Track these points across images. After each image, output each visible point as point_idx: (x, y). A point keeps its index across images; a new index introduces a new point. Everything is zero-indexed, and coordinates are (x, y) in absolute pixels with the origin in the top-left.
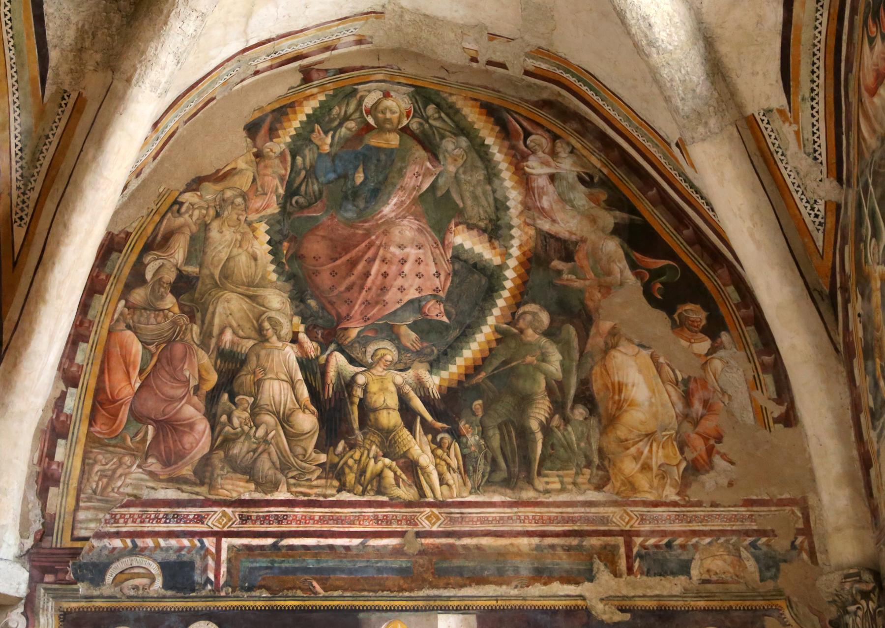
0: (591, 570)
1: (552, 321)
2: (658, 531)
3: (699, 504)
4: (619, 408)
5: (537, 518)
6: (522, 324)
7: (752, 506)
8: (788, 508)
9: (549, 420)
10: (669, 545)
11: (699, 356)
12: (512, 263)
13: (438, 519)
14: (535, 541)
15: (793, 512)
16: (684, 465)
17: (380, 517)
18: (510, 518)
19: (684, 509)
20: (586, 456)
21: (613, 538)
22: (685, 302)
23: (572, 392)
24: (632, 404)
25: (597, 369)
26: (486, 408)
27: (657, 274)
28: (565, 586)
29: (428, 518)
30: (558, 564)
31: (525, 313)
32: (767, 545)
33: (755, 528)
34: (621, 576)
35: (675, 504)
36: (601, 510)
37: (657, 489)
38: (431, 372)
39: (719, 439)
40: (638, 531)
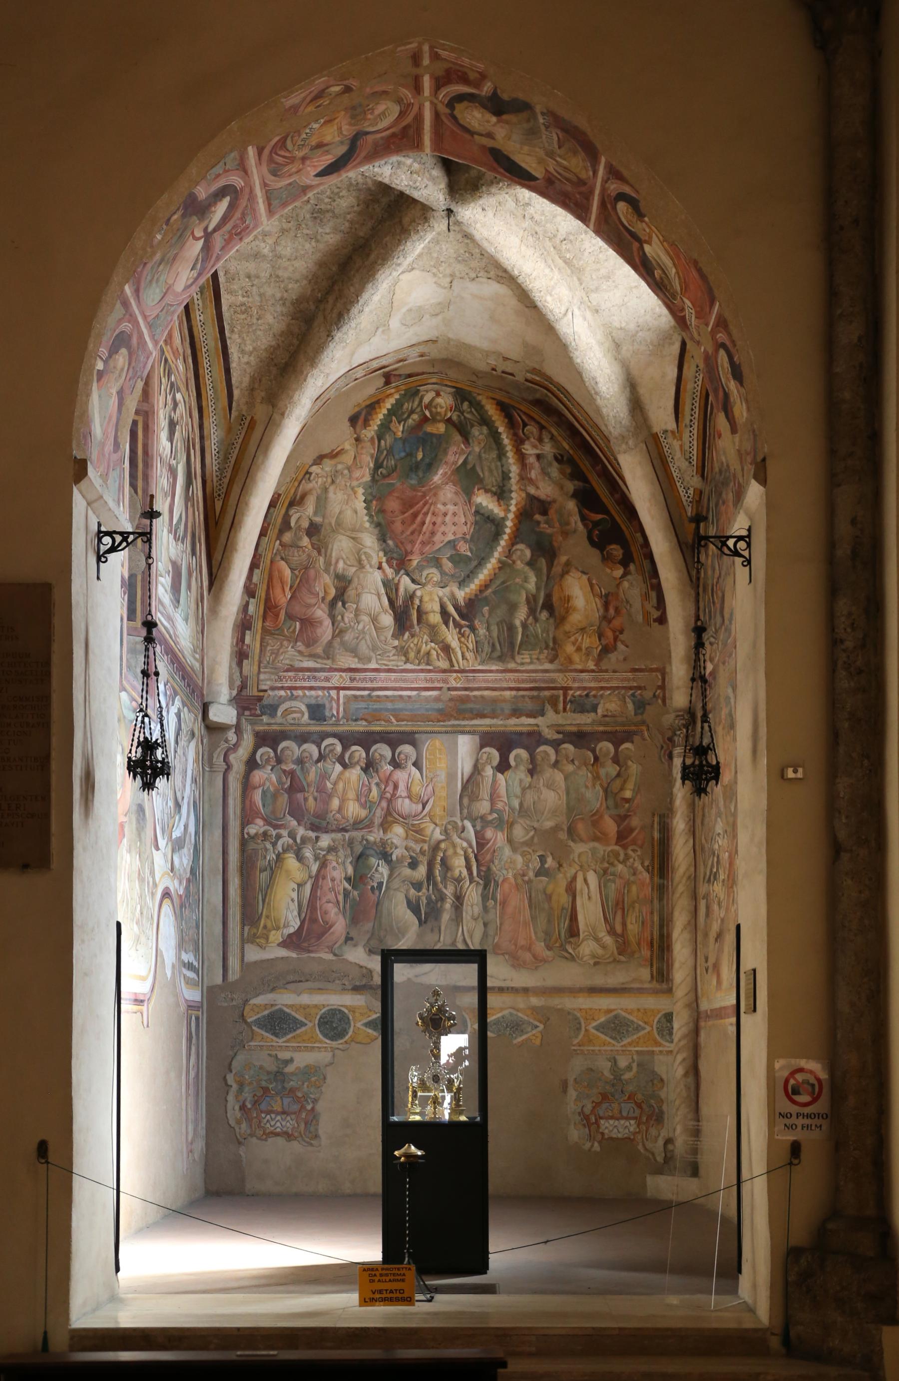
1: (532, 555)
3: (606, 671)
4: (567, 612)
6: (514, 557)
9: (526, 620)
10: (587, 695)
11: (615, 579)
12: (511, 516)
16: (600, 648)
20: (546, 642)
22: (610, 544)
23: (541, 602)
24: (575, 609)
25: (556, 588)
26: (491, 612)
27: (596, 524)
29: (455, 679)
31: (517, 550)
32: (641, 695)
35: (593, 671)
36: (552, 674)
38: (459, 588)
39: (621, 632)
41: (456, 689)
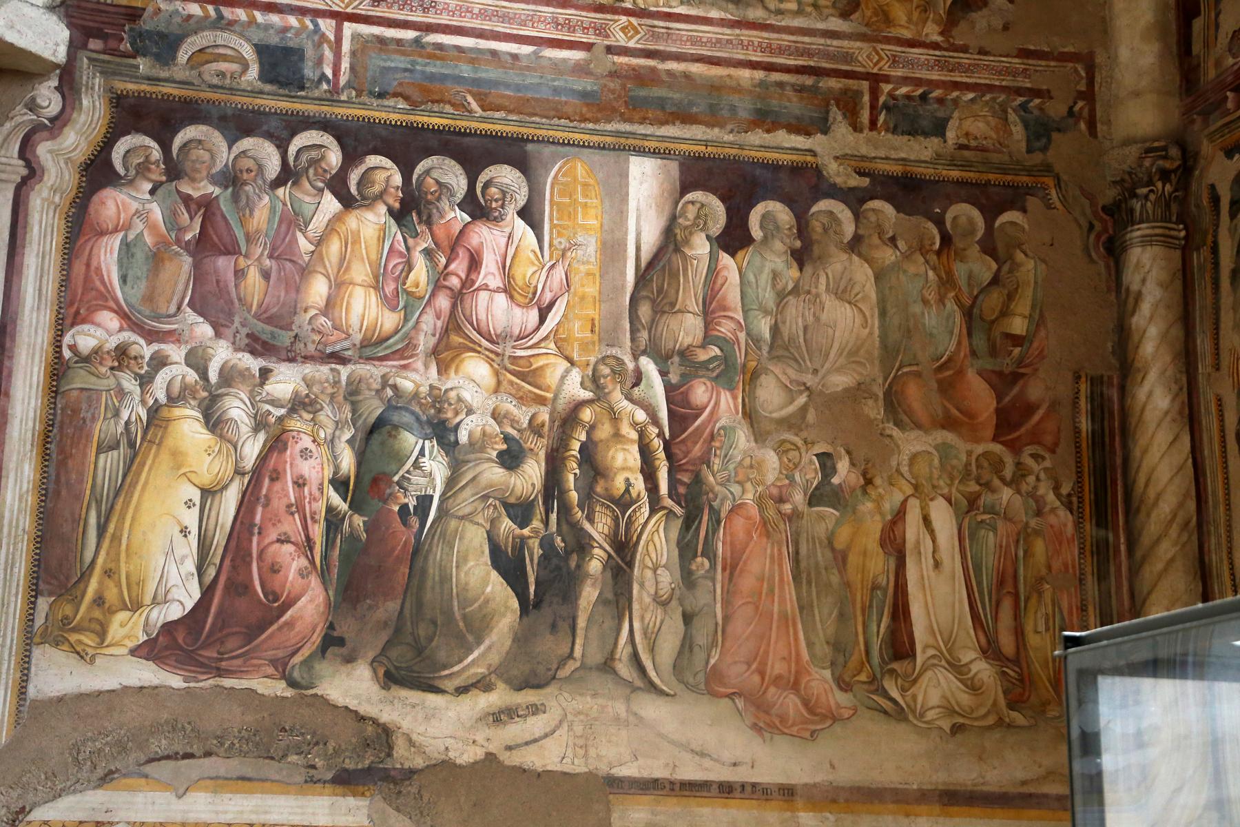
0: (826, 120)
2: (911, 78)
3: (964, 49)
5: (764, 45)
7: (1028, 58)
8: (1071, 65)
10: (923, 97)
13: (637, 32)
14: (759, 75)
15: (1076, 71)
17: (561, 21)
18: (729, 42)
19: (946, 53)
21: (856, 82)
28: (793, 137)
29: (623, 29)
30: (786, 108)
33: (1029, 85)
34: (861, 131)
35: (935, 46)
36: (845, 43)
37: (916, 24)
40: (887, 76)
41: (625, 51)
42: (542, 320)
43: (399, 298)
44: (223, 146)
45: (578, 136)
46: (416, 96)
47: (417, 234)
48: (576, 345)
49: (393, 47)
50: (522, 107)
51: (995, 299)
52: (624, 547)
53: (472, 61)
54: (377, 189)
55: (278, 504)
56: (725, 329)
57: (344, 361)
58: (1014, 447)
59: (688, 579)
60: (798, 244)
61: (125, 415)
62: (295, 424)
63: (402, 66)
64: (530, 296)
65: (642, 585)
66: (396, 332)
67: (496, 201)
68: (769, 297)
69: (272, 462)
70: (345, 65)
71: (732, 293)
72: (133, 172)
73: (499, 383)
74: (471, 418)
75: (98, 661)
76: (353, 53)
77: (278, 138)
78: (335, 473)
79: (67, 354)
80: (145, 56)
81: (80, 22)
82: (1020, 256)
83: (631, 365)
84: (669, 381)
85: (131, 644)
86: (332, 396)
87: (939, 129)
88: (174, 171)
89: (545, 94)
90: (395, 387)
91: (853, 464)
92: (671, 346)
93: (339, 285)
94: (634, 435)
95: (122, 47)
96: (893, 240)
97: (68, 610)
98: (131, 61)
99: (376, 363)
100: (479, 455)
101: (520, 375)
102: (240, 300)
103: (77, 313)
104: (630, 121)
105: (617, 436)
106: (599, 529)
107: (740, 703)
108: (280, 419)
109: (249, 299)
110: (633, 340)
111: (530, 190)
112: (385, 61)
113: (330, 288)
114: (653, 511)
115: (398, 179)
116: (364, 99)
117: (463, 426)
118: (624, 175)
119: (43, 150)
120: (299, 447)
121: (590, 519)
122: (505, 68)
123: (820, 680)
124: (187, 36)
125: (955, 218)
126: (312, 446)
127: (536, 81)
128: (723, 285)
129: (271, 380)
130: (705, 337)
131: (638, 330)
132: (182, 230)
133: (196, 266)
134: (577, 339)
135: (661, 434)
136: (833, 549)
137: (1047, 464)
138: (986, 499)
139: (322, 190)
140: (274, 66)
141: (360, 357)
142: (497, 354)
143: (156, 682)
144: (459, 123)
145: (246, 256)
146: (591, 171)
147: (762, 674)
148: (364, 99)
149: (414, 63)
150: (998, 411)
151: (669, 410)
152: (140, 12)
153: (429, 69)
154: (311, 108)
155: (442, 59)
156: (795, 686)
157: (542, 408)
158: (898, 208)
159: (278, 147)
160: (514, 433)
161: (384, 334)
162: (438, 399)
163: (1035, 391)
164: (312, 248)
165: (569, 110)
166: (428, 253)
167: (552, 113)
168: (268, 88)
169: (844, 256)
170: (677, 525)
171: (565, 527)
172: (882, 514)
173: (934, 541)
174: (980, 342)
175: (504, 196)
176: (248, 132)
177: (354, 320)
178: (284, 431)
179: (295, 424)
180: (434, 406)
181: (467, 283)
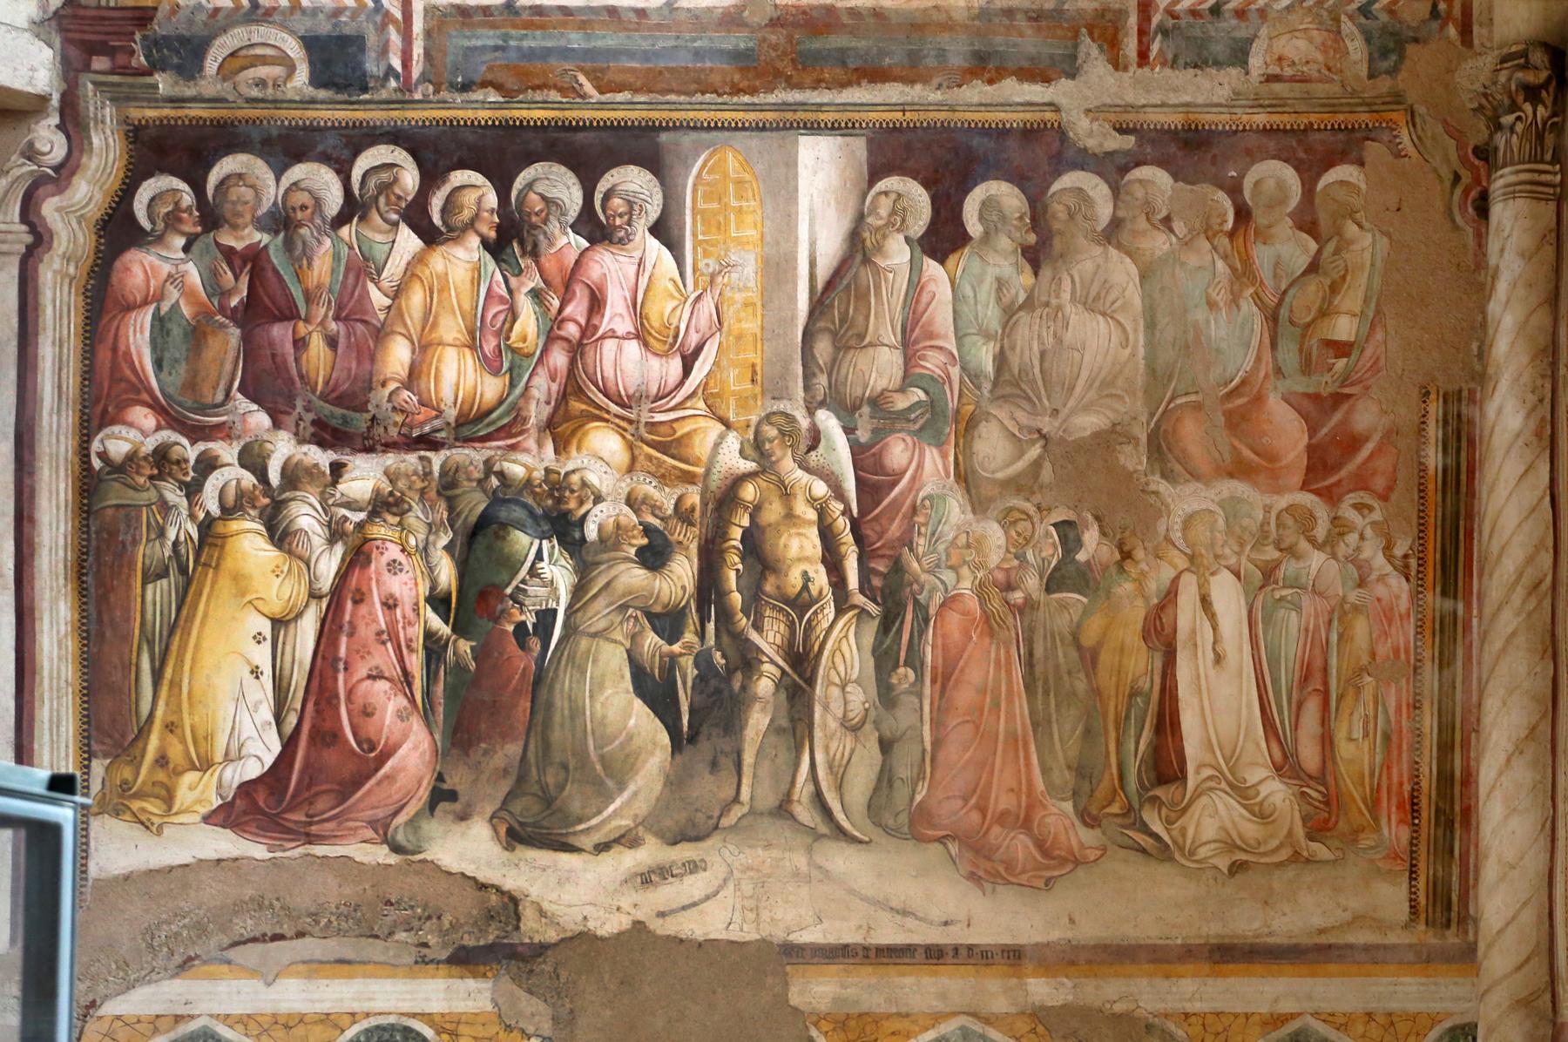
28: (1026, 86)
30: (1015, 45)
42: (687, 371)
43: (506, 361)
44: (268, 176)
45: (728, 115)
46: (511, 83)
47: (521, 271)
48: (732, 402)
49: (478, 18)
50: (650, 82)
51: (1313, 291)
52: (802, 662)
53: (583, 26)
54: (466, 214)
55: (366, 632)
56: (932, 363)
57: (435, 446)
58: (1330, 496)
59: (887, 695)
60: (1032, 238)
61: (172, 534)
62: (378, 531)
63: (491, 43)
64: (670, 340)
65: (826, 707)
66: (501, 402)
67: (621, 216)
68: (991, 315)
69: (353, 582)
70: (418, 50)
71: (941, 314)
72: (161, 225)
73: (633, 459)
74: (600, 506)
75: (167, 831)
76: (428, 34)
77: (337, 161)
78: (433, 588)
79: (97, 463)
80: (163, 70)
81: (77, 36)
82: (1351, 229)
83: (804, 423)
84: (857, 440)
85: (204, 810)
86: (422, 492)
87: (1239, 54)
88: (211, 217)
89: (683, 60)
90: (501, 475)
91: (1103, 533)
92: (859, 392)
93: (424, 348)
94: (812, 515)
95: (134, 63)
96: (1167, 221)
97: (127, 773)
98: (148, 80)
99: (477, 445)
100: (613, 554)
101: (659, 446)
102: (301, 377)
103: (105, 411)
104: (799, 86)
105: (790, 516)
106: (769, 639)
107: (954, 848)
108: (360, 526)
109: (312, 375)
110: (807, 388)
111: (665, 197)
112: (469, 38)
113: (413, 352)
114: (839, 612)
115: (492, 200)
116: (444, 94)
117: (590, 518)
118: (791, 164)
119: (50, 209)
120: (385, 559)
121: (758, 627)
122: (626, 29)
123: (1059, 815)
124: (215, 37)
125: (1257, 184)
126: (401, 558)
127: (672, 43)
128: (929, 304)
129: (346, 476)
130: (905, 377)
131: (814, 375)
132: (226, 294)
133: (246, 339)
134: (734, 393)
135: (847, 512)
136: (1079, 647)
137: (1377, 516)
138: (1289, 568)
139: (395, 225)
140: (327, 63)
141: (456, 439)
142: (630, 422)
143: (235, 853)
144: (568, 114)
145: (307, 321)
146: (746, 163)
147: (983, 811)
148: (444, 94)
149: (506, 38)
150: (1311, 449)
151: (858, 479)
152: (150, 13)
153: (525, 44)
154: (376, 116)
155: (542, 27)
156: (1026, 824)
157: (691, 488)
158: (1176, 176)
159: (338, 172)
160: (656, 522)
161: (485, 407)
162: (557, 485)
163: (1366, 417)
164: (388, 302)
165: (716, 79)
166: (536, 294)
167: (693, 87)
168: (322, 94)
169: (1097, 250)
170: (871, 629)
171: (725, 639)
172: (1146, 599)
173: (1215, 628)
174: (1289, 355)
175: (632, 208)
176: (299, 157)
177: (447, 393)
178: (367, 540)
179: (378, 531)
180: (551, 496)
181: (588, 330)
